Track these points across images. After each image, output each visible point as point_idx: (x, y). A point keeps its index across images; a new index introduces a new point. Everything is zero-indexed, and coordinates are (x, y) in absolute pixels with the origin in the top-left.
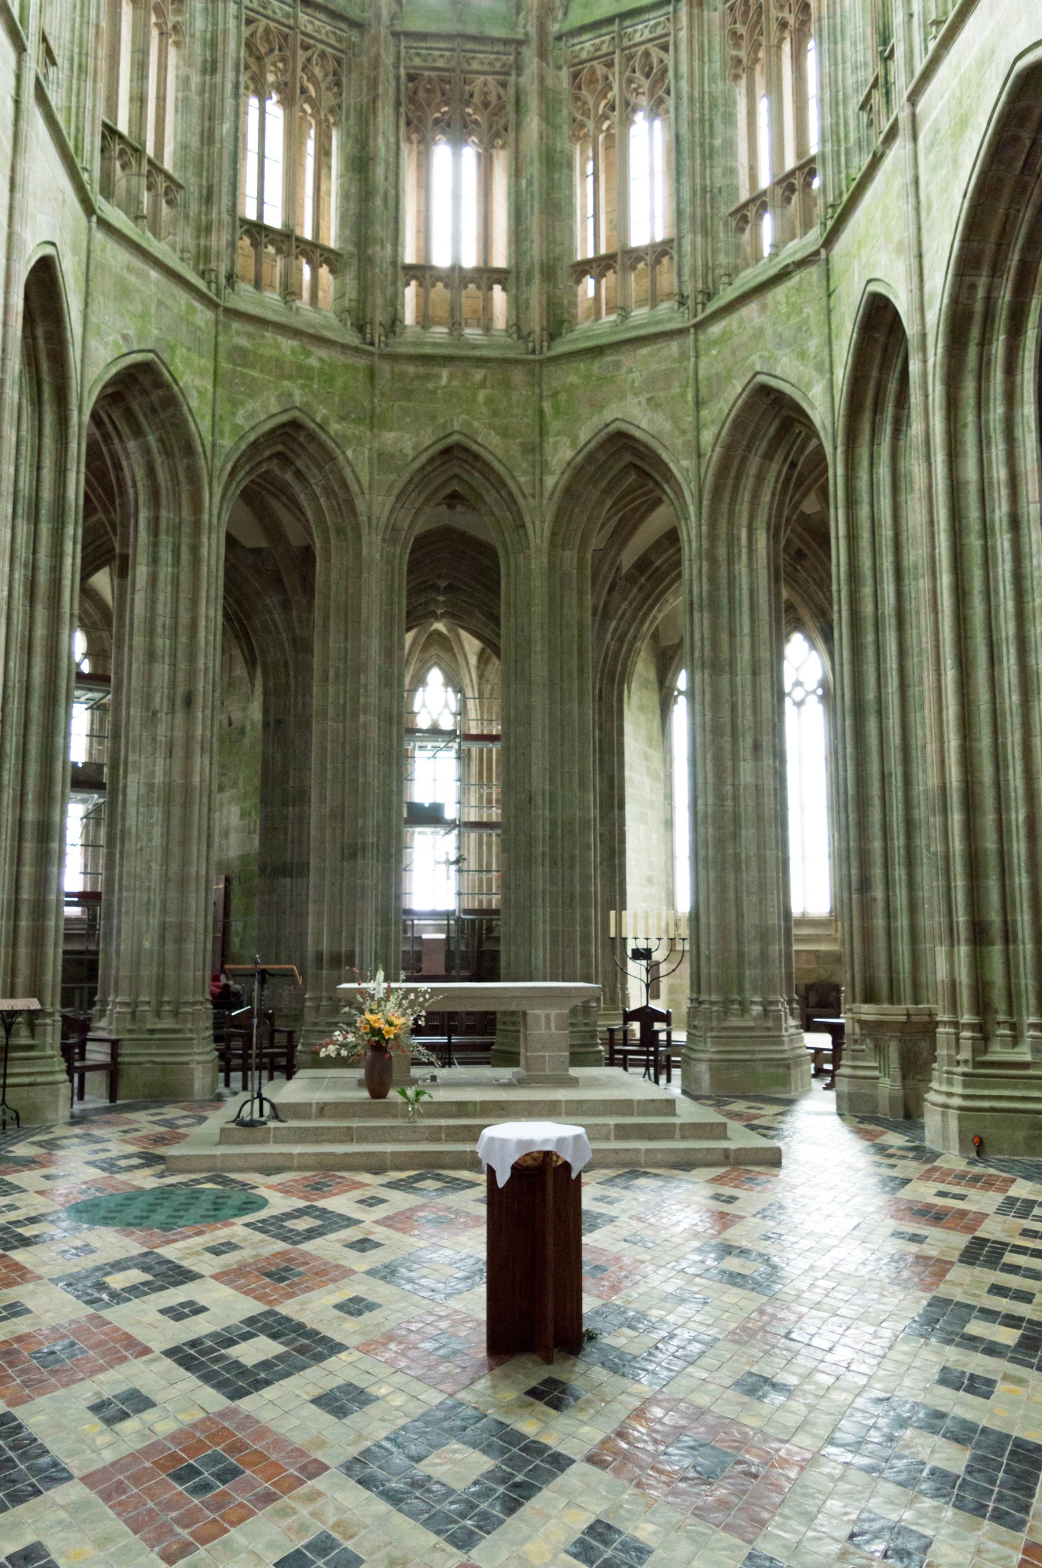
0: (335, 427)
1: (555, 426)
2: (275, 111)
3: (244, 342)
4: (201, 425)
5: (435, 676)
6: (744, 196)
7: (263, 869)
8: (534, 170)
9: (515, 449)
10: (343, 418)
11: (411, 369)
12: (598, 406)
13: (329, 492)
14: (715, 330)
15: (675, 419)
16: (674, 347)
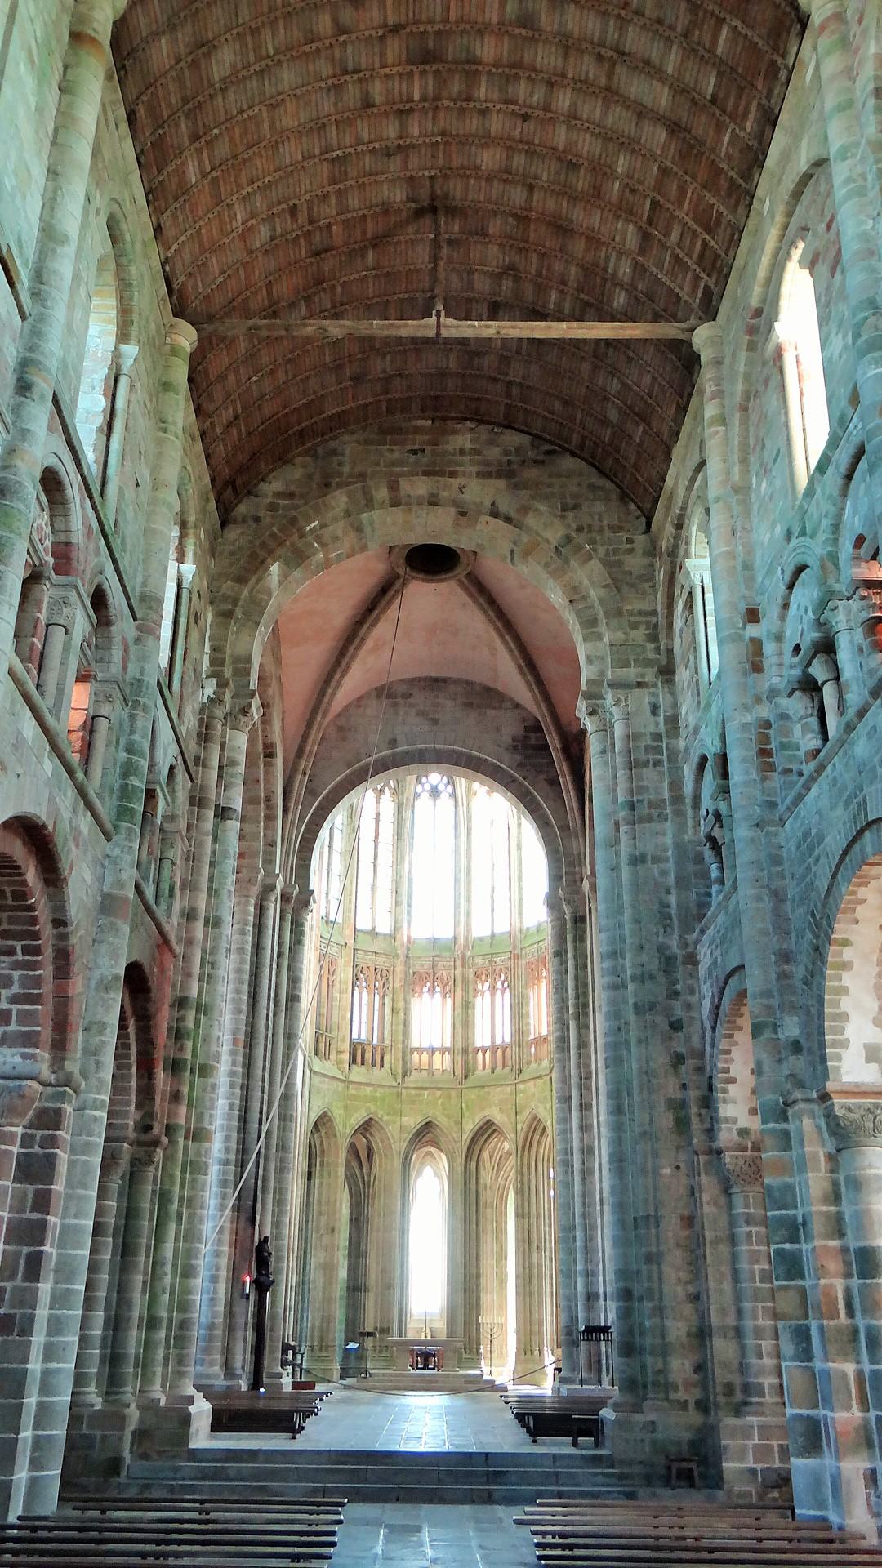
0: (385, 1118)
1: (466, 1114)
2: (365, 994)
3: (353, 1092)
4: (339, 1128)
5: (428, 1171)
6: (532, 1037)
7: (348, 1288)
8: (459, 1011)
9: (452, 1124)
10: (388, 1114)
11: (413, 1092)
12: (482, 1109)
13: (382, 1141)
14: (522, 1086)
15: (509, 1118)
16: (509, 1088)
